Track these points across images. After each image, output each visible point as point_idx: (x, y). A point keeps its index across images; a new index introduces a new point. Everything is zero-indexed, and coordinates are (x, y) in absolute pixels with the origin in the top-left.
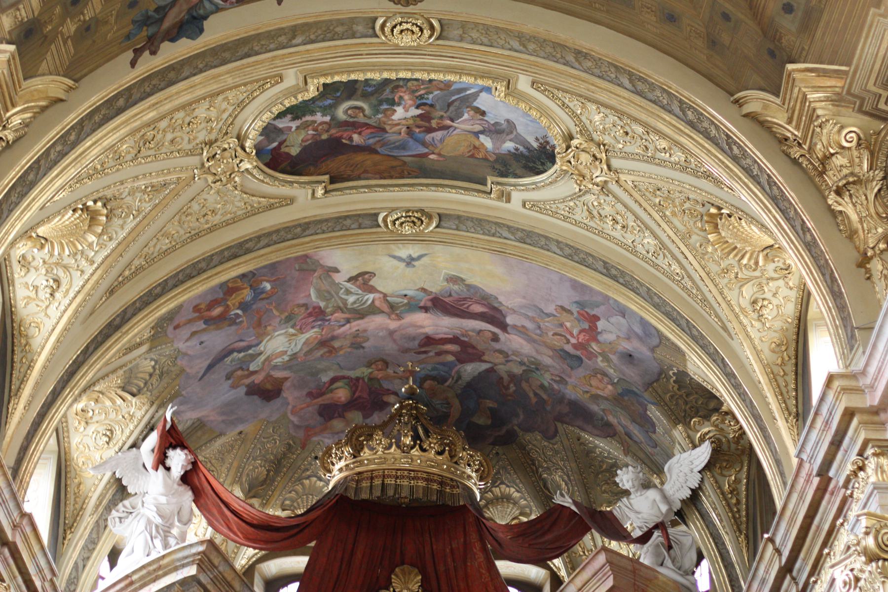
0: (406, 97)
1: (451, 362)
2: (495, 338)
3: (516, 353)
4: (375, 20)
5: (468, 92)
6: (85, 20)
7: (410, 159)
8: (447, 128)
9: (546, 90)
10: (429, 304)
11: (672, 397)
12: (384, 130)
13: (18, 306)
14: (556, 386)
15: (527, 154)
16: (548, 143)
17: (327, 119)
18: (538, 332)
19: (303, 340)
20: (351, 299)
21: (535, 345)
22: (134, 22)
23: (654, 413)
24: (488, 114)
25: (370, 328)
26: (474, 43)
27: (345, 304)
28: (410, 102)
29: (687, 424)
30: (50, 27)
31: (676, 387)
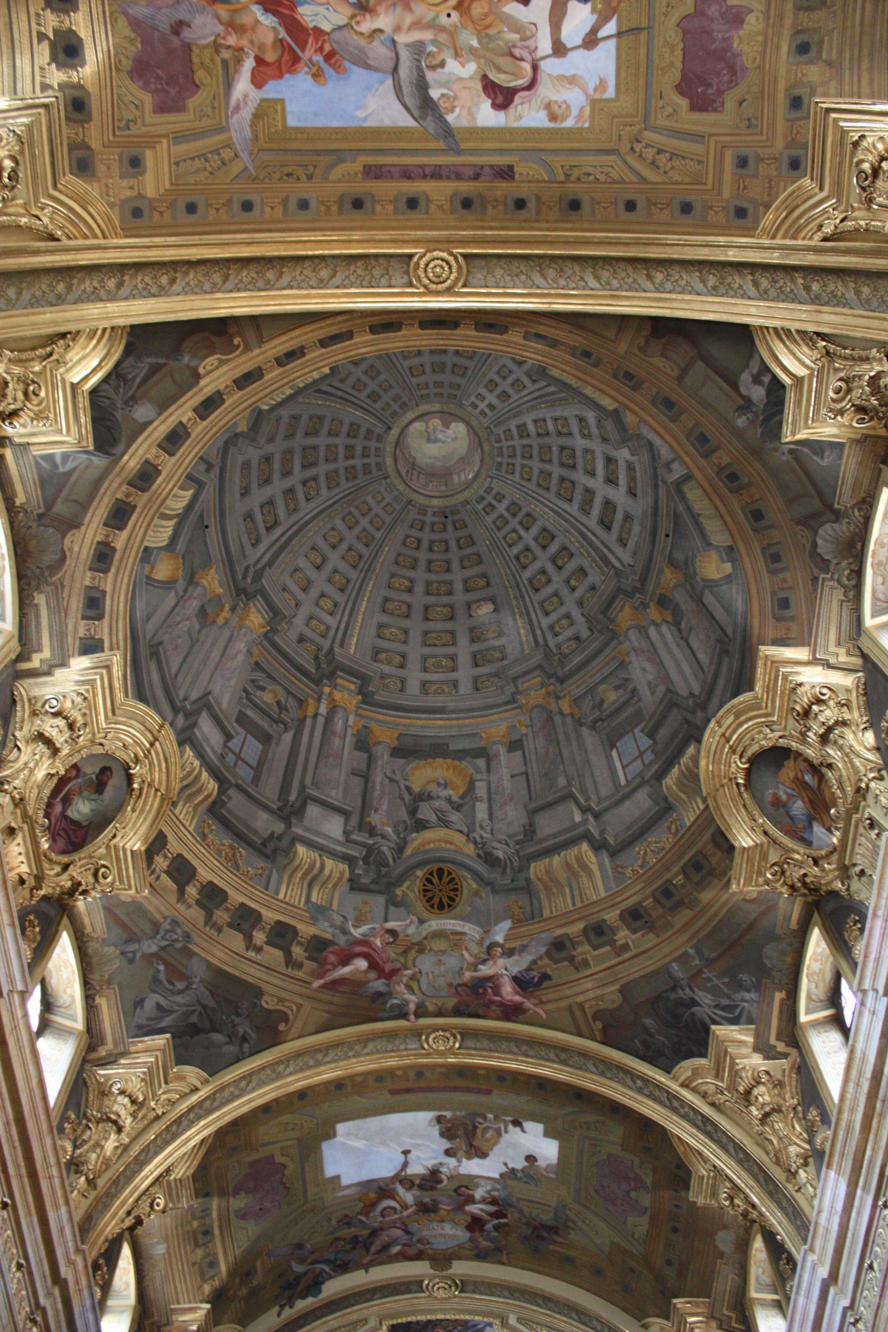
4: (422, 1282)
26: (481, 1293)
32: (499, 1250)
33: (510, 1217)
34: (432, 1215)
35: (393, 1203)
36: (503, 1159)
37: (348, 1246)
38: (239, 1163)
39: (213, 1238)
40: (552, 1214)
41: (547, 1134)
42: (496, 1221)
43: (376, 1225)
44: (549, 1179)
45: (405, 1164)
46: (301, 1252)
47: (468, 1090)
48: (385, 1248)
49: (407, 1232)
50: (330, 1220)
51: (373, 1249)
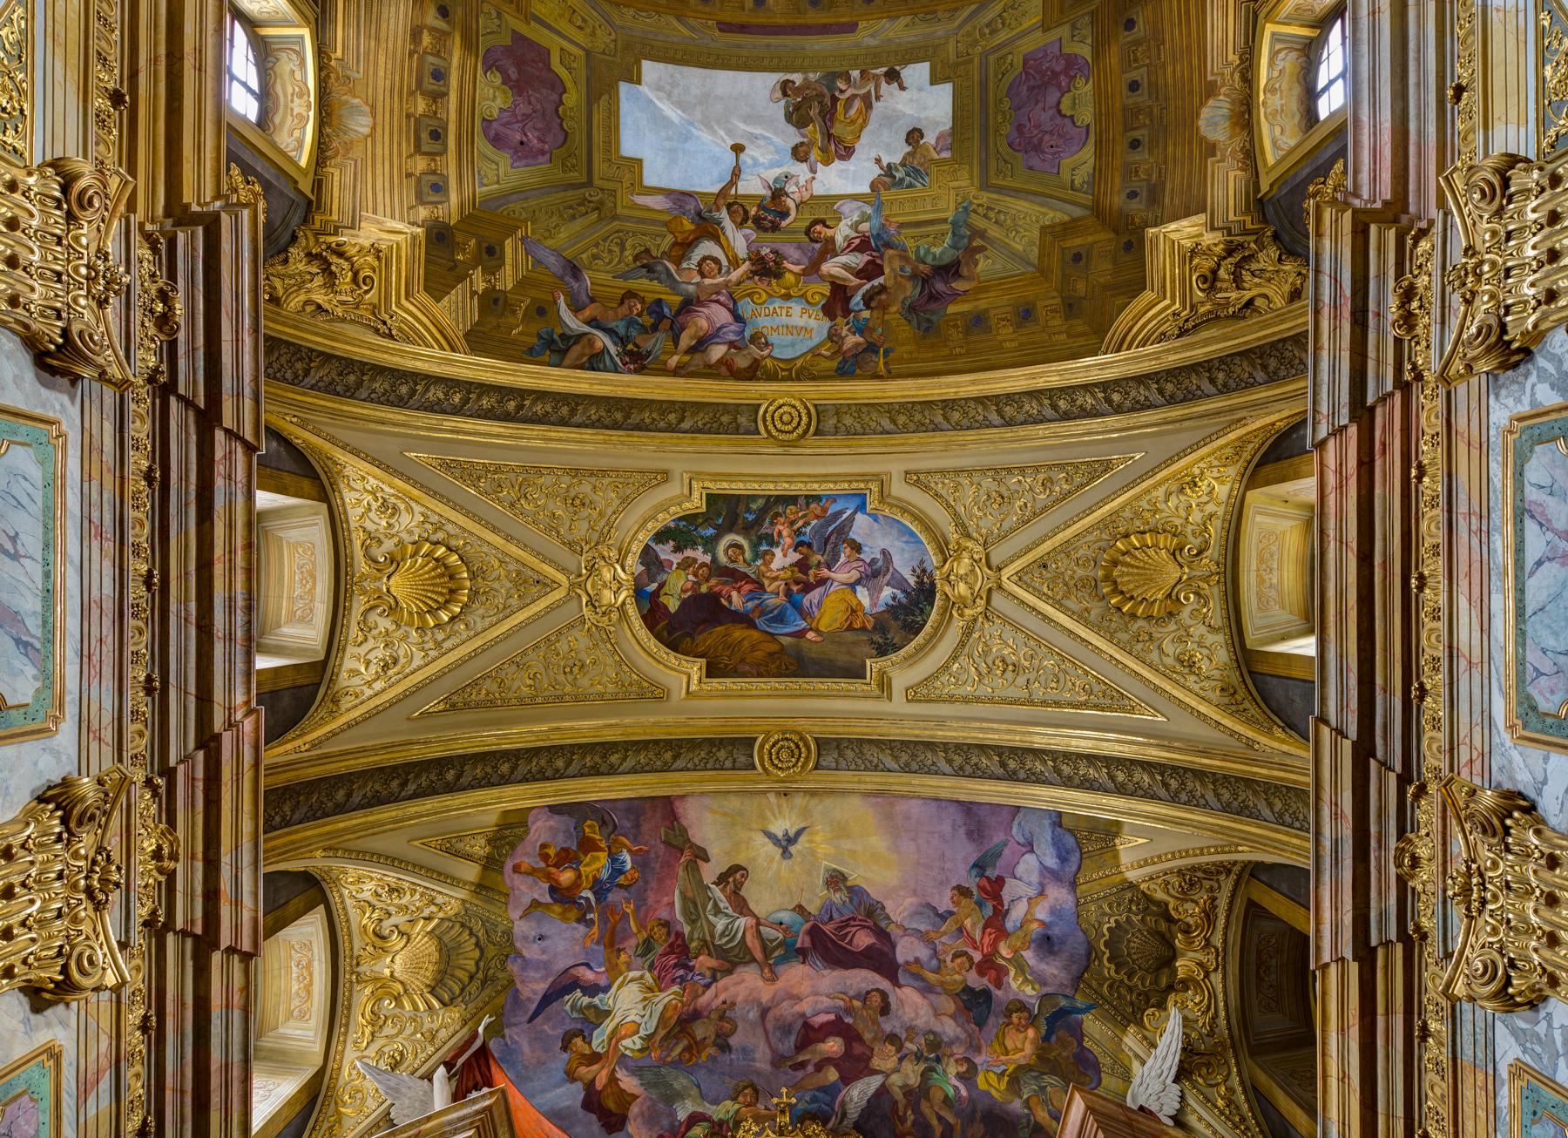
0: (785, 533)
1: (834, 1084)
2: (885, 1009)
3: (911, 1030)
5: (845, 516)
6: (494, 287)
7: (789, 639)
8: (822, 582)
9: (918, 480)
10: (808, 944)
11: (1110, 987)
12: (762, 586)
13: (341, 677)
14: (964, 1093)
15: (904, 601)
16: (924, 571)
17: (707, 559)
18: (934, 962)
19: (660, 1007)
20: (720, 924)
21: (932, 997)
22: (540, 337)
23: (1094, 1027)
24: (865, 549)
25: (740, 999)
27: (712, 936)
28: (788, 540)
29: (1140, 1024)
30: (460, 257)
31: (1113, 967)
32: (872, 348)
33: (887, 270)
34: (774, 281)
35: (716, 251)
36: (873, 155)
37: (647, 320)
38: (499, 16)
39: (445, 151)
40: (948, 239)
41: (934, 80)
42: (868, 286)
43: (691, 288)
44: (944, 162)
45: (736, 173)
46: (575, 285)
47: (825, 30)
48: (701, 344)
49: (738, 318)
50: (623, 249)
51: (686, 340)
